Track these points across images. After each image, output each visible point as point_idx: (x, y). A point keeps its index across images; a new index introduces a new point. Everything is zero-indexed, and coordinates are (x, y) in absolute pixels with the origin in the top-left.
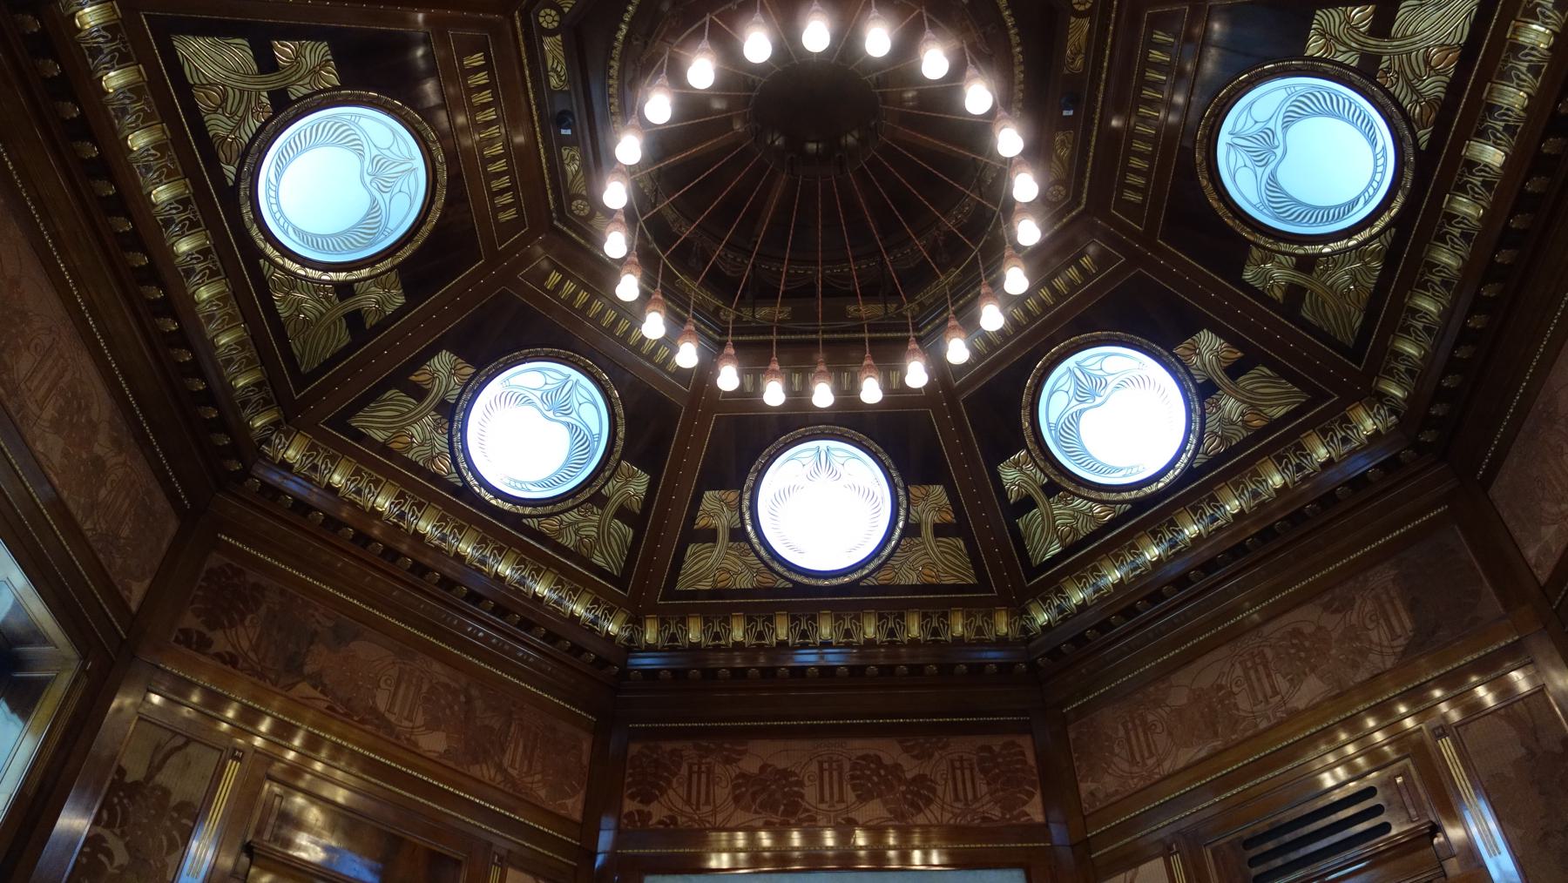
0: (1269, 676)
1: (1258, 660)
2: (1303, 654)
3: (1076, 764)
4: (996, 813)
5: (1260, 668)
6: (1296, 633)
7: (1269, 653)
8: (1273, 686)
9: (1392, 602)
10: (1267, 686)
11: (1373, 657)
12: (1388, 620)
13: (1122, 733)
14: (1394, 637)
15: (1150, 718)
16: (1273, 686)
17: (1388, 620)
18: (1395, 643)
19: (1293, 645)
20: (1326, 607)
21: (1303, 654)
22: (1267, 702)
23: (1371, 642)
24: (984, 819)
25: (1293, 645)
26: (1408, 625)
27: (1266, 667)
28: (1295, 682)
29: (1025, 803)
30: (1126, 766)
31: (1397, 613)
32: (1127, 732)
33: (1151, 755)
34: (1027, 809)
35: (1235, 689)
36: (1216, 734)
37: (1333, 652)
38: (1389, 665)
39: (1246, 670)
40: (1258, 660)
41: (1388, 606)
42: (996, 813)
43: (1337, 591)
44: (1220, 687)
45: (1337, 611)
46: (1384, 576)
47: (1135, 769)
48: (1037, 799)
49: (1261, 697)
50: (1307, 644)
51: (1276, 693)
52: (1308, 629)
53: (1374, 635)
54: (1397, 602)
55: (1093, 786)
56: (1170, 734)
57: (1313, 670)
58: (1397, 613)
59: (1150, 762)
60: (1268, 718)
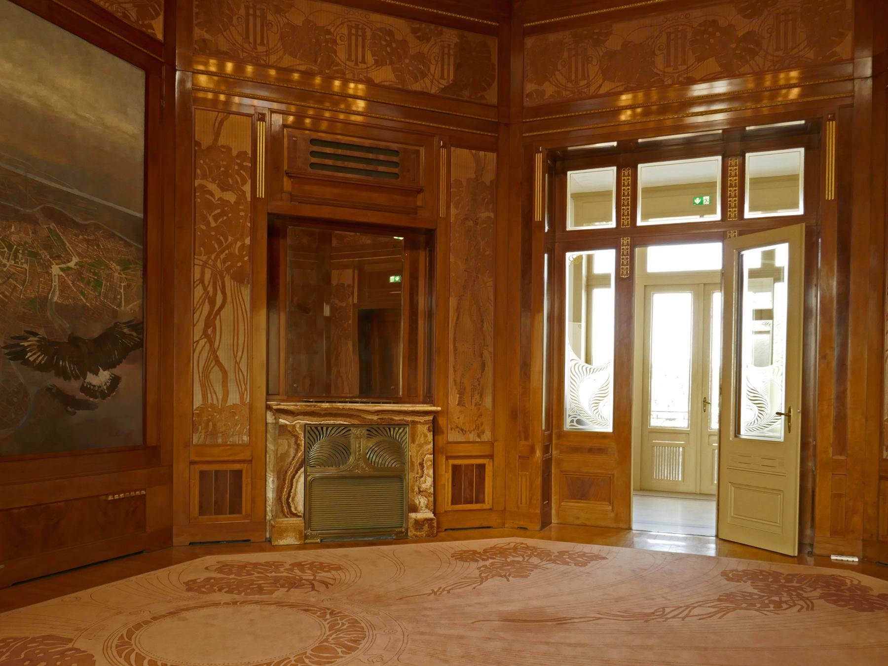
0: (363, 47)
1: (360, 33)
2: (388, 49)
3: (195, 10)
4: (133, 15)
5: (360, 39)
6: (390, 33)
7: (369, 34)
8: (363, 56)
9: (449, 55)
10: (360, 56)
11: (427, 81)
12: (443, 65)
13: (242, 12)
14: (442, 77)
15: (270, 17)
16: (363, 56)
17: (443, 65)
18: (441, 81)
19: (386, 40)
20: (414, 31)
21: (388, 49)
22: (356, 64)
23: (429, 71)
24: (125, 16)
25: (386, 40)
26: (452, 77)
27: (363, 40)
28: (379, 63)
29: (153, 18)
30: (240, 39)
31: (449, 65)
32: (248, 14)
33: (262, 44)
34: (153, 23)
35: (338, 41)
36: (316, 61)
37: (407, 61)
38: (433, 91)
39: (350, 35)
40: (360, 33)
41: (446, 57)
42: (133, 15)
43: (423, 26)
44: (328, 32)
45: (418, 38)
46: (451, 36)
47: (246, 45)
48: (161, 18)
49: (353, 58)
50: (394, 45)
51: (363, 62)
52: (398, 36)
53: (432, 69)
54: (452, 58)
55: (207, 36)
56: (282, 38)
57: (392, 63)
58: (449, 65)
59: (261, 49)
60: (354, 75)
